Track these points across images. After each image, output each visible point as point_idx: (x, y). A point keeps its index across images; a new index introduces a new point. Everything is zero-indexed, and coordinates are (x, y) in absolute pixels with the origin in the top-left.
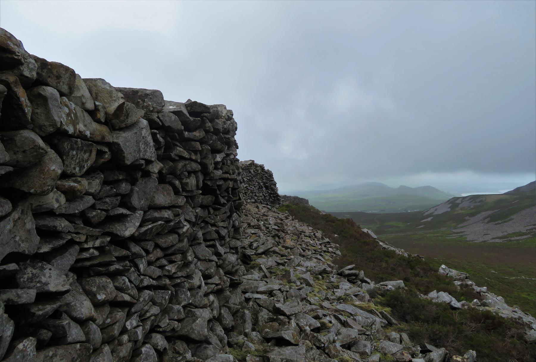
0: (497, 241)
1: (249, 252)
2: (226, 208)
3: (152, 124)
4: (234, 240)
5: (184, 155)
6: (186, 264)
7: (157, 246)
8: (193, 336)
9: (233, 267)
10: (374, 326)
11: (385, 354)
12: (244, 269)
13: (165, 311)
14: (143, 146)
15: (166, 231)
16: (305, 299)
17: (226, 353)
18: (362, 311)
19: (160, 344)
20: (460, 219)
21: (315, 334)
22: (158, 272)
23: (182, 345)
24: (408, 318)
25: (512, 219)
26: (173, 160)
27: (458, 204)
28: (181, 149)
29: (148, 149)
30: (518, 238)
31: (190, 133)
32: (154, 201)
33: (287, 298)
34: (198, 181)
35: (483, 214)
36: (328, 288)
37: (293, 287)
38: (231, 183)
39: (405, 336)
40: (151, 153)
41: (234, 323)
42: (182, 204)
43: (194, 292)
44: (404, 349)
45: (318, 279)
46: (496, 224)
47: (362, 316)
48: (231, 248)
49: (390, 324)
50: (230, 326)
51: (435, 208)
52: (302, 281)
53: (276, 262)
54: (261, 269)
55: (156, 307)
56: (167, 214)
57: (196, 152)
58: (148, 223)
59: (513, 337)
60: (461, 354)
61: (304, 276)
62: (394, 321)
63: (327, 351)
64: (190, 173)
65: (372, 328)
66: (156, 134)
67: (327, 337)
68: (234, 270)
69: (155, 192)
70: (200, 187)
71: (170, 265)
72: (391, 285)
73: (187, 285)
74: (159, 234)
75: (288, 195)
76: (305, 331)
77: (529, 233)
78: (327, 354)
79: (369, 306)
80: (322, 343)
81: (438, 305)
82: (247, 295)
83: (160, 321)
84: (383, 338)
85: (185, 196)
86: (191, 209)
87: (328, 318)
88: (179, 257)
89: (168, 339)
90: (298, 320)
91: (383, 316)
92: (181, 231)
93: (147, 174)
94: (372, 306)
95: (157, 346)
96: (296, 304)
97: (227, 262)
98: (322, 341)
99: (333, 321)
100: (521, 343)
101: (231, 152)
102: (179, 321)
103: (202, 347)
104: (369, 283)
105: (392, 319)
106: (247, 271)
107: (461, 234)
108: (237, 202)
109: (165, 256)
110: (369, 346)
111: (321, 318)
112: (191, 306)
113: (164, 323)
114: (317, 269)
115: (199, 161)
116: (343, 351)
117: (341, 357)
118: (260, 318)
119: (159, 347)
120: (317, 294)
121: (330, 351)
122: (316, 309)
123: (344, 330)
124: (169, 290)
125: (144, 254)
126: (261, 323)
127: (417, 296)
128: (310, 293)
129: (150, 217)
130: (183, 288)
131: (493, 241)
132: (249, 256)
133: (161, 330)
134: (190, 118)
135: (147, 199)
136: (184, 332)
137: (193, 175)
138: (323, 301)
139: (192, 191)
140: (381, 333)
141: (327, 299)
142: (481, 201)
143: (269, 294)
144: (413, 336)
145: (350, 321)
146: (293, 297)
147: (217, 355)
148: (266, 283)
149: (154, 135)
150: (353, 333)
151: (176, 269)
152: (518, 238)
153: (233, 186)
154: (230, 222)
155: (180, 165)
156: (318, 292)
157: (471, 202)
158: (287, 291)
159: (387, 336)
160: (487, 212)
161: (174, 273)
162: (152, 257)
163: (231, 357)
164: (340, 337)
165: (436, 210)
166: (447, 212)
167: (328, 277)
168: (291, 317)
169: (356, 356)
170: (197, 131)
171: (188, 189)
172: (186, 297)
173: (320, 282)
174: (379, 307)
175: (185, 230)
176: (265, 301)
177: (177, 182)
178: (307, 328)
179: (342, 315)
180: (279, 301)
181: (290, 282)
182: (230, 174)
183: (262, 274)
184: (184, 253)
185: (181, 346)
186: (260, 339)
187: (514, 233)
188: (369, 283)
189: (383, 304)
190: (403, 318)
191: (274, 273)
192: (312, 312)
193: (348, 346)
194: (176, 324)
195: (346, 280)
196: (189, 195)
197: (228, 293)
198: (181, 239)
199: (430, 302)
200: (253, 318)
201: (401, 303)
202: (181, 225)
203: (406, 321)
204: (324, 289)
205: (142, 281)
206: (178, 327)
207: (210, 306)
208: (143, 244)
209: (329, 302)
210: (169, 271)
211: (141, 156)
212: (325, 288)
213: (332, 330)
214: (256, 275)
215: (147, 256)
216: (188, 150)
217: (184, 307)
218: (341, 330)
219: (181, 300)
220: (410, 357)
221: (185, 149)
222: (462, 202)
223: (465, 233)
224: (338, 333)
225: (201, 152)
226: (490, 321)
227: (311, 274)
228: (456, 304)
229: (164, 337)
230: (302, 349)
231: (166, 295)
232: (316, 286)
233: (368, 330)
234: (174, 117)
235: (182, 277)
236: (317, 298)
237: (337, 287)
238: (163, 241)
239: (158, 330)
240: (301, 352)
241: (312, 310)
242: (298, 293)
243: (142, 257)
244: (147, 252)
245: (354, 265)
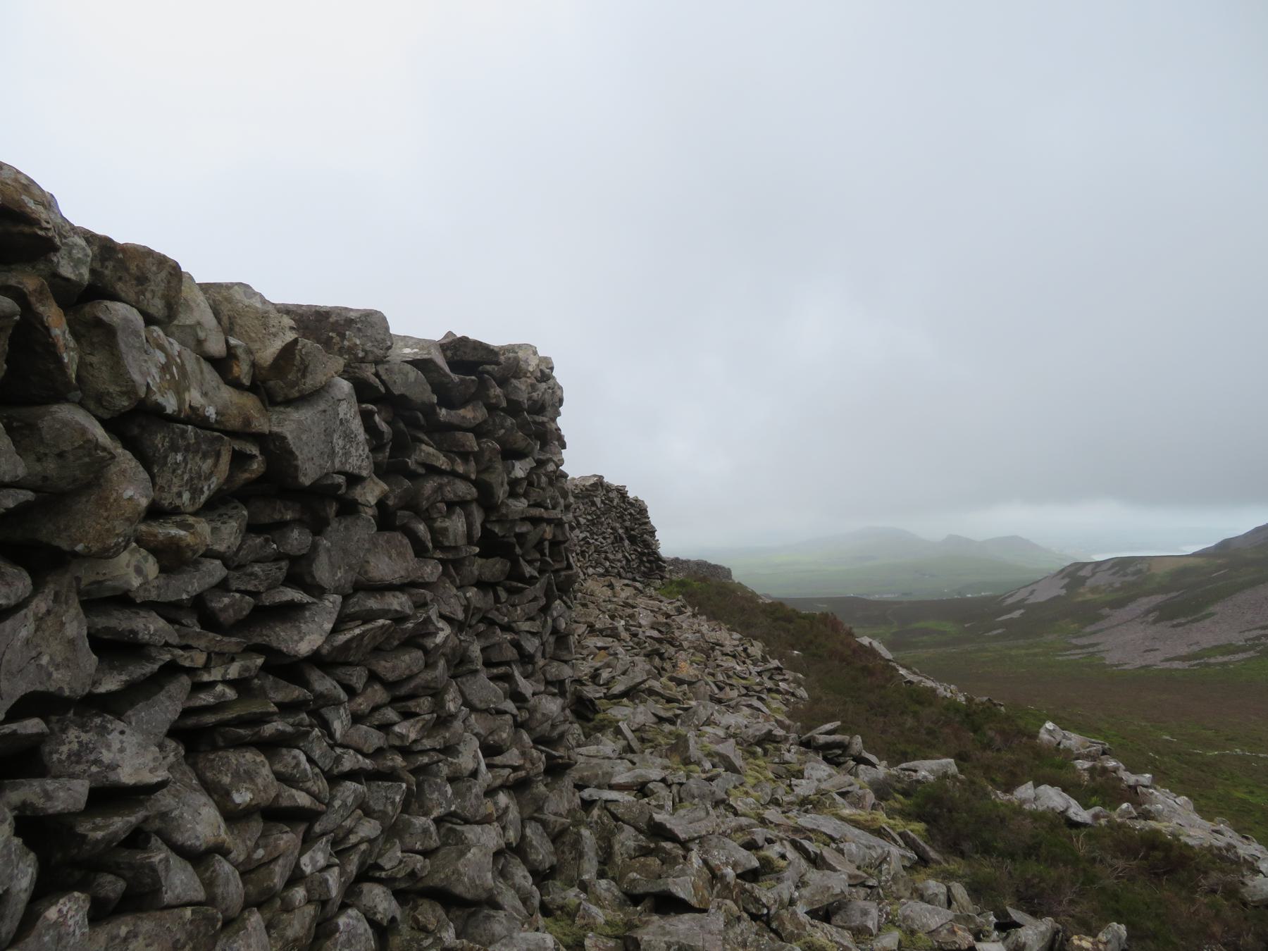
0: (1176, 665)
1: (591, 692)
2: (537, 589)
3: (363, 391)
4: (555, 664)
5: (438, 464)
6: (444, 721)
7: (374, 677)
8: (459, 890)
9: (553, 726)
10: (885, 866)
11: (913, 932)
12: (580, 731)
13: (393, 831)
14: (341, 442)
15: (396, 643)
16: (723, 801)
17: (537, 930)
18: (857, 831)
19: (380, 908)
20: (1088, 614)
21: (747, 886)
22: (376, 740)
23: (434, 911)
24: (966, 846)
25: (1212, 614)
26: (412, 476)
27: (1086, 578)
28: (431, 450)
29: (353, 450)
30: (1226, 659)
31: (453, 413)
32: (366, 572)
33: (681, 800)
34: (470, 526)
35: (1145, 603)
36: (778, 777)
37: (695, 775)
38: (548, 529)
39: (959, 890)
40: (359, 459)
41: (555, 860)
42: (434, 579)
43: (462, 786)
44: (957, 919)
45: (754, 754)
46: (1174, 626)
47: (858, 843)
48: (548, 683)
49: (923, 861)
50: (547, 865)
51: (1034, 587)
52: (716, 760)
53: (655, 715)
54: (618, 732)
55: (373, 821)
56: (397, 602)
57: (465, 456)
58: (352, 624)
59: (1214, 891)
60: (1091, 932)
61: (720, 748)
62: (933, 854)
63: (774, 925)
64: (451, 505)
65: (880, 872)
66: (371, 413)
67: (775, 891)
68: (555, 734)
69: (369, 550)
70: (475, 540)
71: (407, 723)
72: (926, 769)
73: (445, 770)
74: (378, 650)
75: (683, 557)
76: (723, 876)
77: (1252, 648)
78: (775, 932)
79: (873, 820)
80: (764, 906)
81: (1037, 817)
82: (586, 794)
83: (380, 855)
84: (907, 894)
85: (441, 561)
86: (455, 591)
87: (777, 847)
88: (426, 702)
89: (401, 896)
90: (706, 852)
91: (906, 843)
92: (430, 643)
93: (349, 508)
94: (882, 819)
95: (375, 914)
96: (703, 814)
97: (538, 716)
98: (764, 900)
99: (788, 855)
100: (1234, 906)
101: (549, 456)
102: (426, 853)
103: (481, 916)
104: (874, 765)
105: (928, 849)
106: (587, 736)
107: (1091, 650)
108: (563, 573)
109: (394, 701)
110: (874, 912)
111: (761, 848)
112: (455, 820)
113: (390, 860)
114: (750, 731)
115: (473, 477)
116: (812, 926)
117: (809, 939)
118: (617, 847)
119: (379, 916)
120: (751, 791)
121: (782, 923)
122: (750, 826)
123: (814, 876)
124: (402, 780)
125: (343, 696)
126: (618, 860)
127: (986, 795)
128: (735, 787)
129: (357, 608)
130: (436, 776)
131: (1167, 665)
132: (591, 701)
133: (383, 874)
134: (452, 375)
135: (351, 567)
136: (437, 880)
137: (458, 510)
138: (765, 806)
139: (456, 548)
140: (901, 883)
141: (775, 802)
142: (1139, 572)
143: (639, 791)
144: (976, 891)
145: (828, 854)
146: (694, 797)
147: (515, 935)
148: (630, 765)
149: (366, 417)
150: (837, 882)
151: (418, 732)
152: (1226, 659)
153: (554, 536)
154: (546, 621)
155: (429, 486)
156: (754, 786)
157: (1114, 574)
158: (681, 784)
159: (916, 890)
161: (415, 741)
162: (362, 704)
163: (549, 940)
164: (806, 892)
165: (1032, 593)
166: (1059, 596)
167: (778, 750)
168: (691, 845)
169: (842, 937)
170: (469, 408)
171: (447, 544)
172: (441, 798)
173: (758, 762)
174: (899, 822)
175: (439, 638)
176: (629, 808)
177: (421, 528)
178: (729, 871)
179: (810, 839)
180: (661, 807)
181: (687, 761)
182: (546, 508)
183: (623, 743)
184: (437, 694)
185: (430, 913)
186: (617, 897)
187: (1217, 647)
188: (874, 765)
189: (907, 816)
190: (953, 848)
191: (650, 741)
192: (740, 834)
193: (824, 914)
194: (418, 861)
195: (820, 758)
196: (450, 556)
197: (542, 788)
198: (431, 661)
199: (1018, 810)
200: (600, 847)
201: (950, 811)
202: (432, 629)
203: (962, 855)
204: (768, 780)
205: (338, 760)
206: (423, 867)
207: (499, 819)
208: (340, 672)
209: (779, 810)
210: (402, 737)
211: (337, 465)
212: (771, 776)
213: (786, 874)
214: (608, 745)
215: (349, 700)
216: (447, 452)
217: (438, 821)
218: (808, 876)
219: (430, 805)
220: (971, 938)
221: (439, 449)
222: (1094, 574)
223: (1101, 647)
224: (801, 884)
225: (478, 456)
226: (1159, 854)
227: (737, 743)
228: (1080, 814)
229: (390, 892)
230: (716, 920)
231: (396, 793)
232: (750, 772)
233: (871, 875)
234: (413, 374)
235: (434, 749)
236: (751, 800)
237: (799, 774)
238: (388, 665)
239: (377, 874)
240: (714, 928)
241: (741, 829)
242: (706, 787)
243: (337, 703)
244: (351, 692)
245: (839, 723)
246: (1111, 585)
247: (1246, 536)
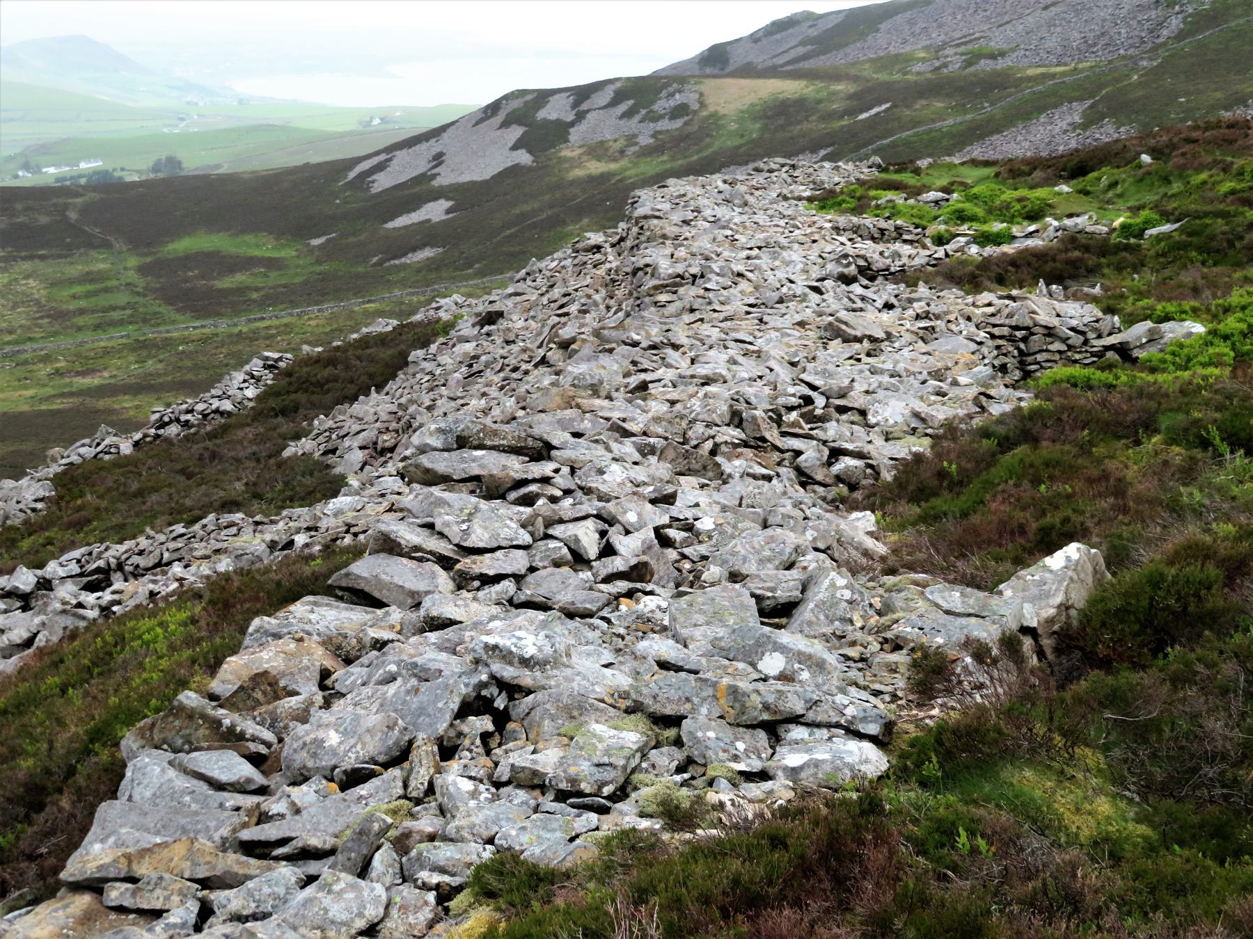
27: (560, 131)
51: (433, 147)
142: (680, 111)
157: (628, 114)
165: (438, 158)
222: (580, 116)
246: (631, 139)
247: (755, 38)
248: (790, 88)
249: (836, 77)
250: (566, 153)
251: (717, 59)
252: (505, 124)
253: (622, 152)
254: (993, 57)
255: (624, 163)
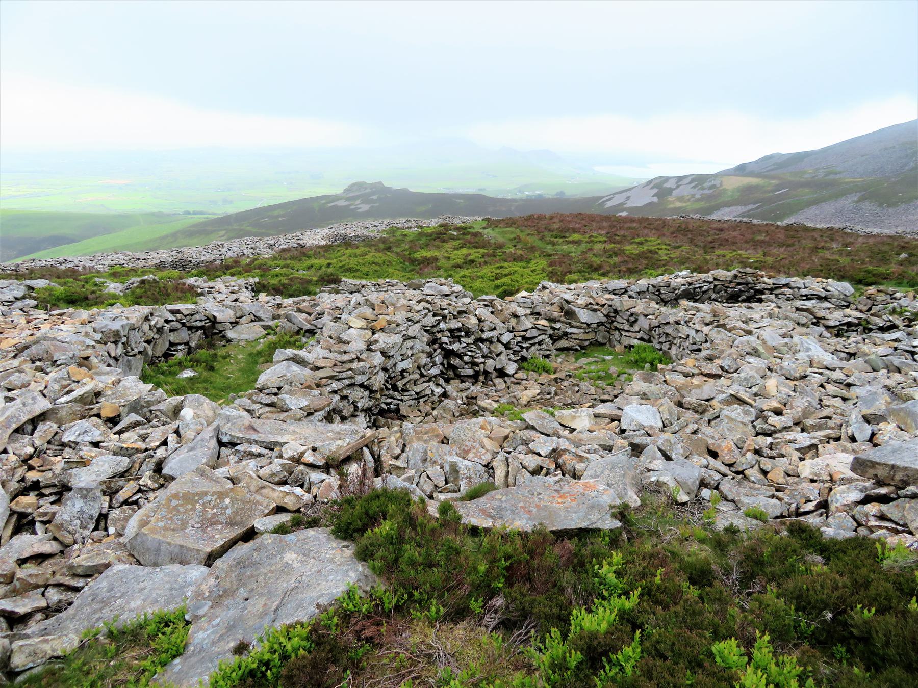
27: (670, 191)
51: (628, 194)
142: (714, 186)
157: (694, 187)
160: (733, 208)
165: (628, 198)
166: (651, 204)
222: (678, 187)
246: (693, 196)
247: (757, 162)
248: (754, 181)
249: (773, 178)
250: (670, 199)
251: (741, 170)
252: (652, 188)
253: (689, 200)
254: (836, 174)
255: (689, 203)
